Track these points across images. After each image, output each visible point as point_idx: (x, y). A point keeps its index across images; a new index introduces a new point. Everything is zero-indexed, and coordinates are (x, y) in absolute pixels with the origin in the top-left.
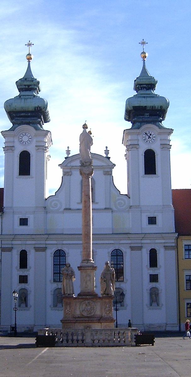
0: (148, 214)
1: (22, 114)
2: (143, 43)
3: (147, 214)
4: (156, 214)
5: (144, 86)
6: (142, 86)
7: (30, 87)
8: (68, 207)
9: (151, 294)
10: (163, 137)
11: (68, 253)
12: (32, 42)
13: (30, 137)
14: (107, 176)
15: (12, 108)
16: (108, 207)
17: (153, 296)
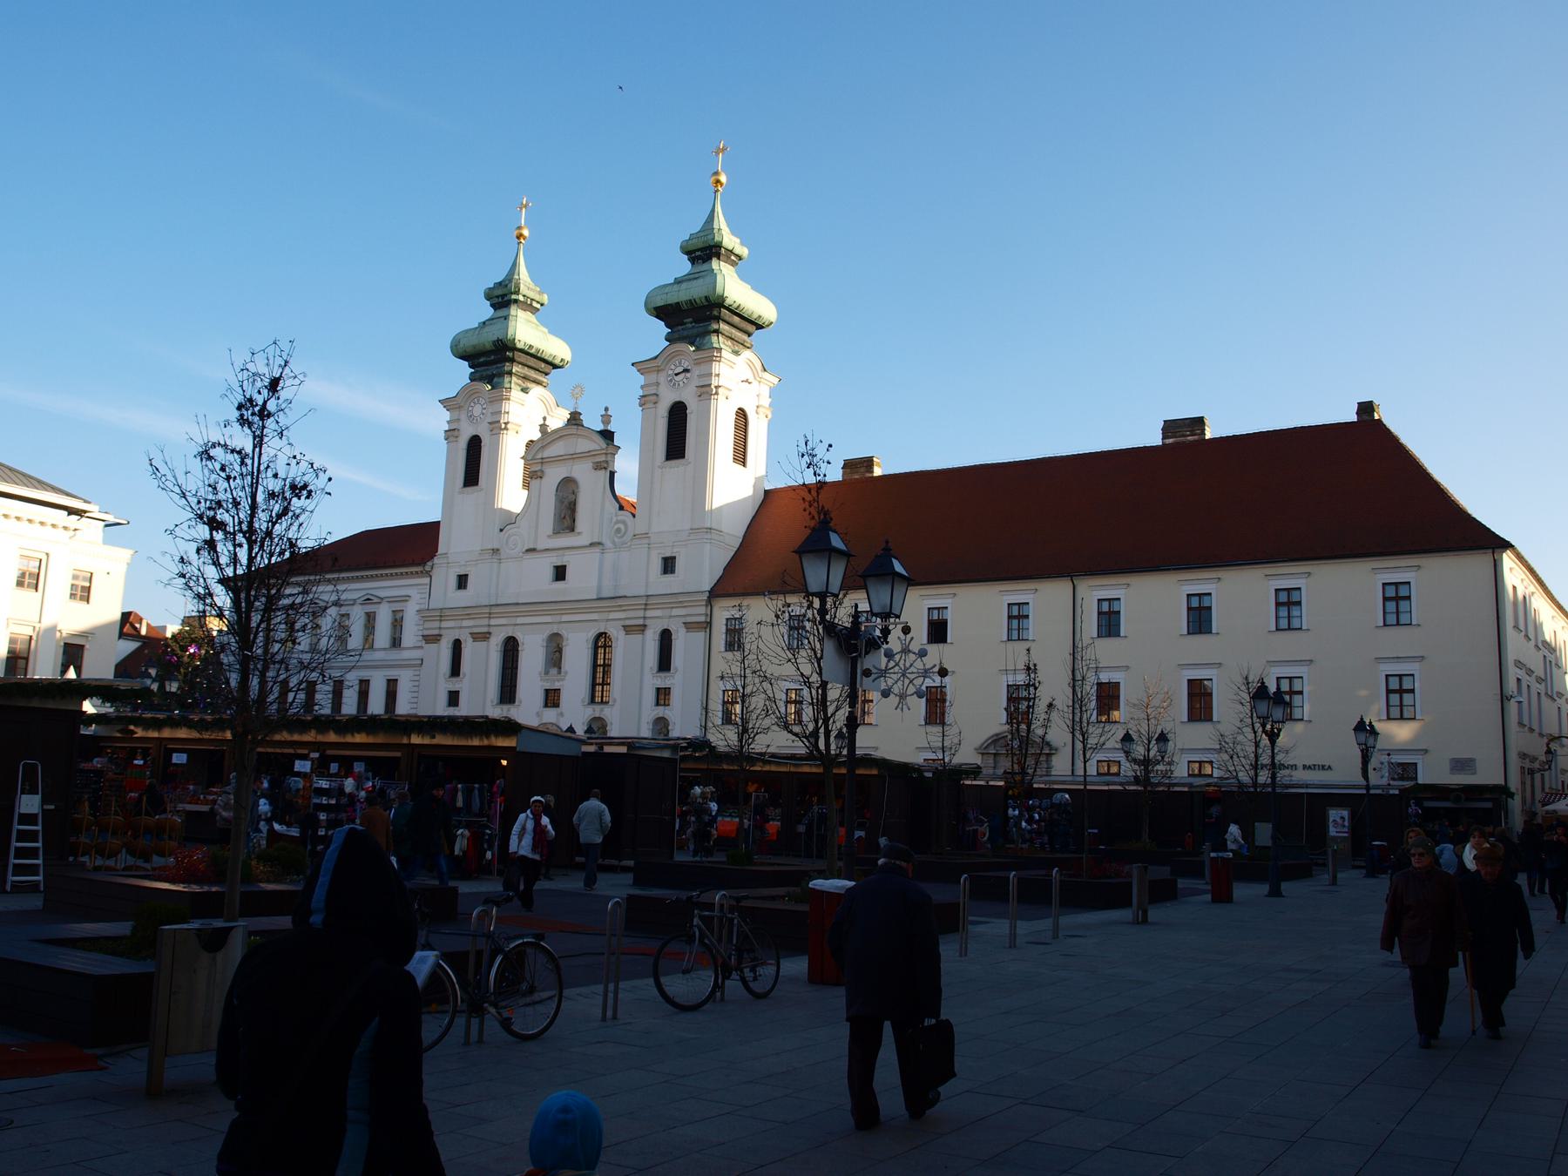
1: (482, 360)
3: (659, 551)
4: (675, 550)
5: (698, 253)
7: (506, 299)
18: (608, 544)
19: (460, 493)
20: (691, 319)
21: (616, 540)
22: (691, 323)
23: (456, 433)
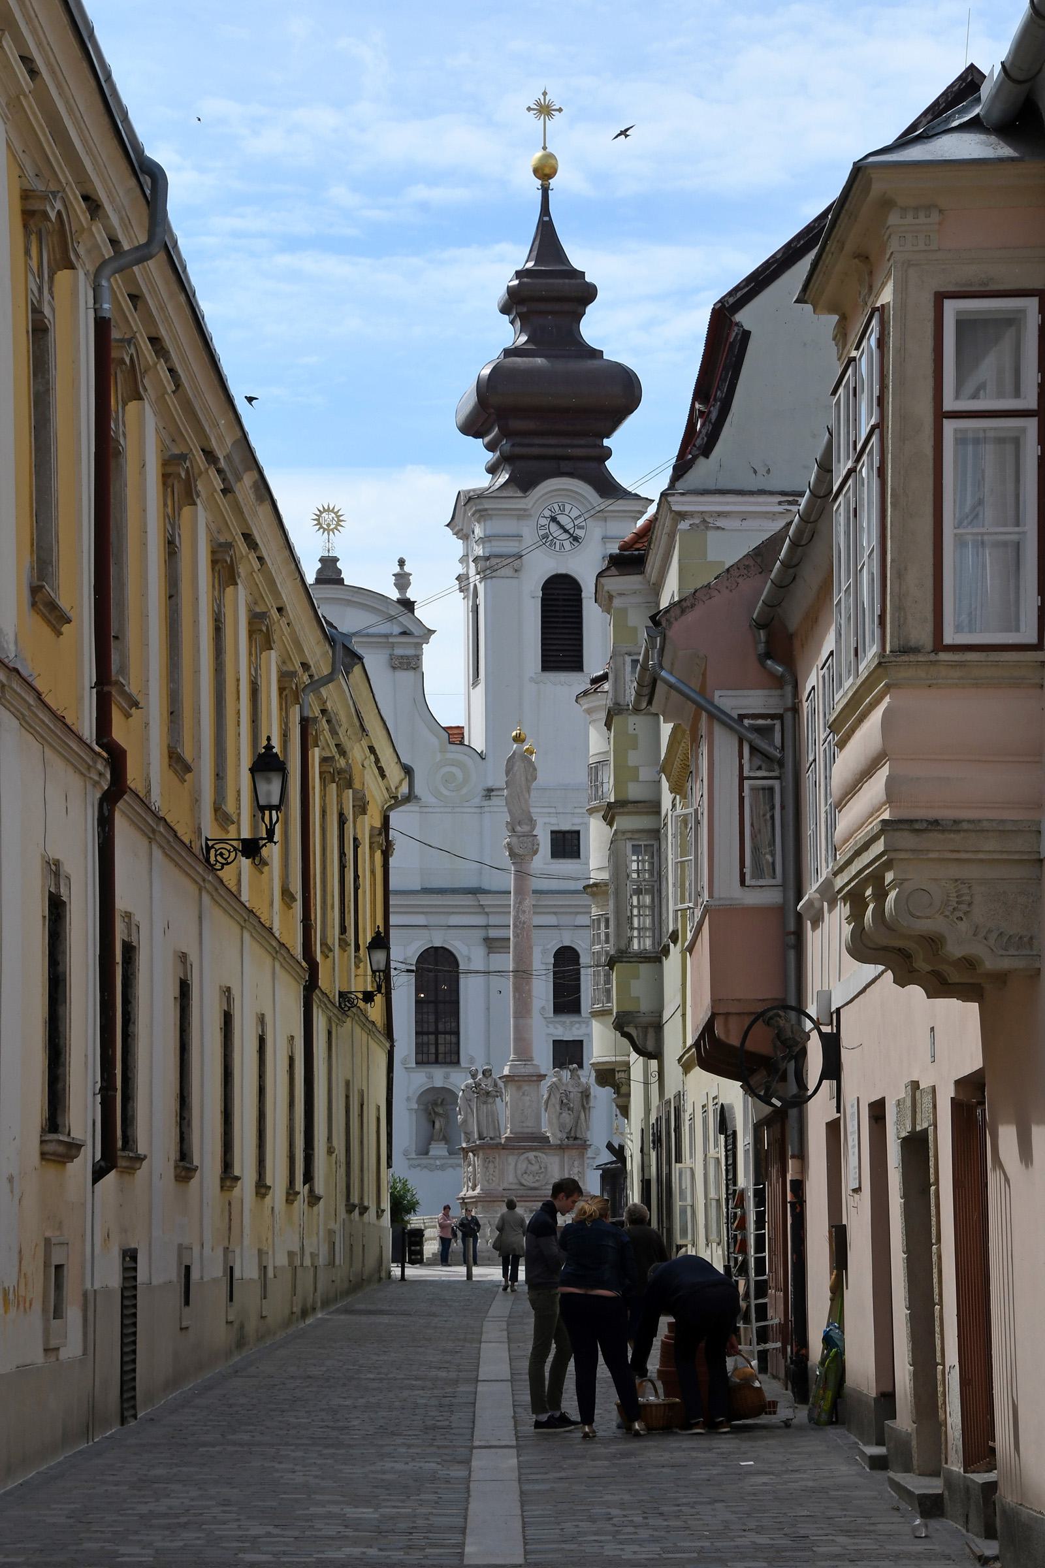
0: (553, 820)
2: (545, 110)
21: (445, 792)
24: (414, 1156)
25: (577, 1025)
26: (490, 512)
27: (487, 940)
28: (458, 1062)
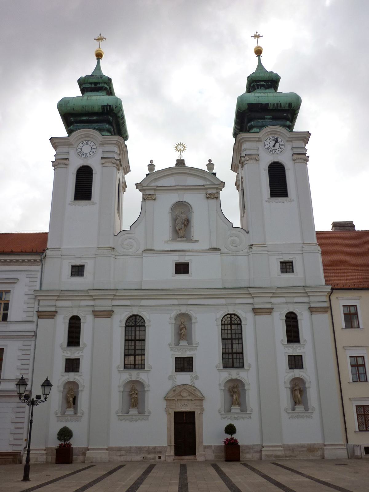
0: (281, 257)
1: (84, 118)
6: (259, 83)
7: (98, 86)
8: (149, 247)
9: (293, 390)
10: (296, 144)
11: (149, 321)
12: (104, 35)
13: (94, 147)
14: (210, 201)
15: (69, 108)
16: (214, 246)
17: (296, 392)
18: (224, 250)
19: (71, 204)
20: (270, 117)
22: (269, 119)
23: (67, 162)
24: (223, 413)
25: (299, 348)
26: (245, 139)
27: (254, 309)
28: (243, 367)
